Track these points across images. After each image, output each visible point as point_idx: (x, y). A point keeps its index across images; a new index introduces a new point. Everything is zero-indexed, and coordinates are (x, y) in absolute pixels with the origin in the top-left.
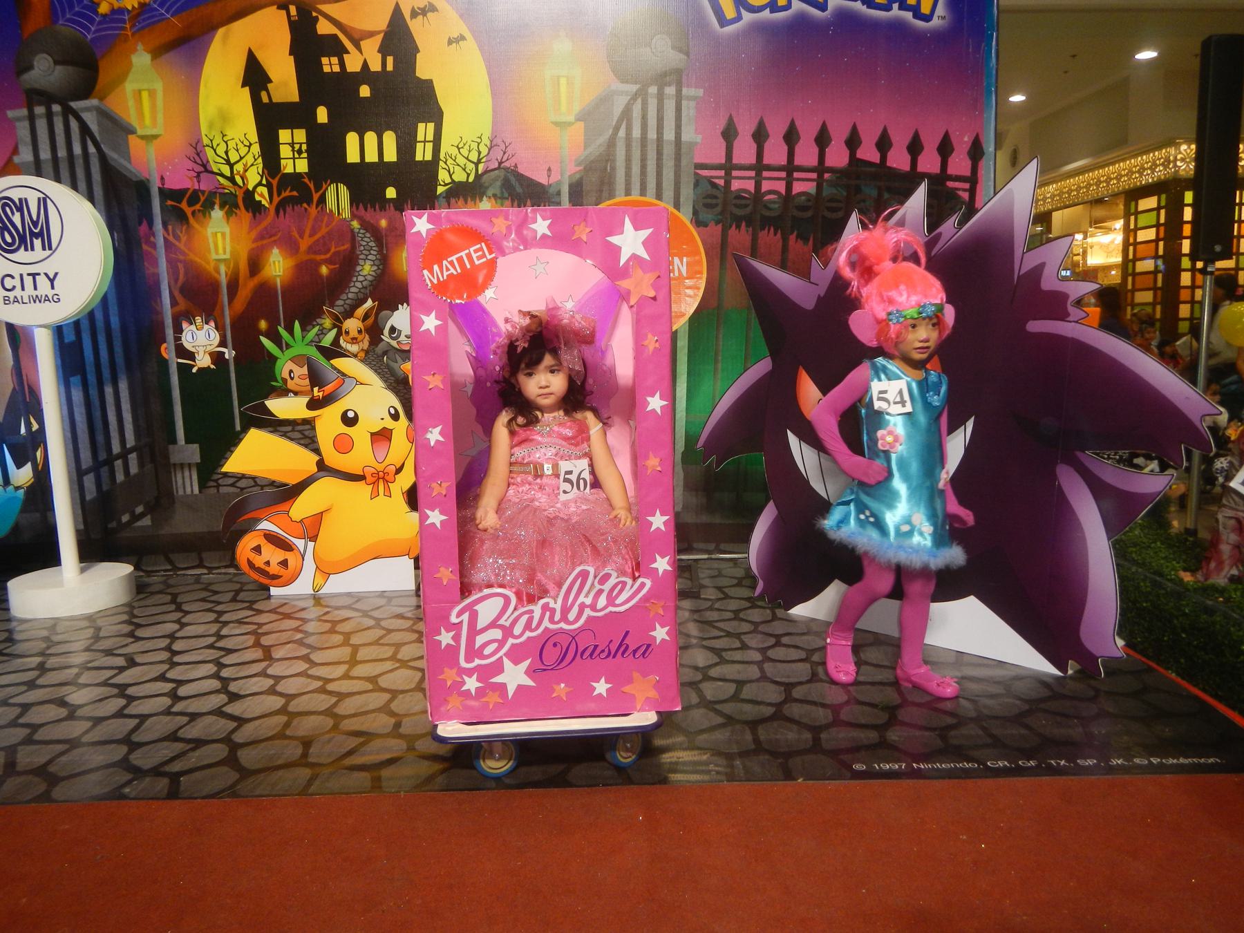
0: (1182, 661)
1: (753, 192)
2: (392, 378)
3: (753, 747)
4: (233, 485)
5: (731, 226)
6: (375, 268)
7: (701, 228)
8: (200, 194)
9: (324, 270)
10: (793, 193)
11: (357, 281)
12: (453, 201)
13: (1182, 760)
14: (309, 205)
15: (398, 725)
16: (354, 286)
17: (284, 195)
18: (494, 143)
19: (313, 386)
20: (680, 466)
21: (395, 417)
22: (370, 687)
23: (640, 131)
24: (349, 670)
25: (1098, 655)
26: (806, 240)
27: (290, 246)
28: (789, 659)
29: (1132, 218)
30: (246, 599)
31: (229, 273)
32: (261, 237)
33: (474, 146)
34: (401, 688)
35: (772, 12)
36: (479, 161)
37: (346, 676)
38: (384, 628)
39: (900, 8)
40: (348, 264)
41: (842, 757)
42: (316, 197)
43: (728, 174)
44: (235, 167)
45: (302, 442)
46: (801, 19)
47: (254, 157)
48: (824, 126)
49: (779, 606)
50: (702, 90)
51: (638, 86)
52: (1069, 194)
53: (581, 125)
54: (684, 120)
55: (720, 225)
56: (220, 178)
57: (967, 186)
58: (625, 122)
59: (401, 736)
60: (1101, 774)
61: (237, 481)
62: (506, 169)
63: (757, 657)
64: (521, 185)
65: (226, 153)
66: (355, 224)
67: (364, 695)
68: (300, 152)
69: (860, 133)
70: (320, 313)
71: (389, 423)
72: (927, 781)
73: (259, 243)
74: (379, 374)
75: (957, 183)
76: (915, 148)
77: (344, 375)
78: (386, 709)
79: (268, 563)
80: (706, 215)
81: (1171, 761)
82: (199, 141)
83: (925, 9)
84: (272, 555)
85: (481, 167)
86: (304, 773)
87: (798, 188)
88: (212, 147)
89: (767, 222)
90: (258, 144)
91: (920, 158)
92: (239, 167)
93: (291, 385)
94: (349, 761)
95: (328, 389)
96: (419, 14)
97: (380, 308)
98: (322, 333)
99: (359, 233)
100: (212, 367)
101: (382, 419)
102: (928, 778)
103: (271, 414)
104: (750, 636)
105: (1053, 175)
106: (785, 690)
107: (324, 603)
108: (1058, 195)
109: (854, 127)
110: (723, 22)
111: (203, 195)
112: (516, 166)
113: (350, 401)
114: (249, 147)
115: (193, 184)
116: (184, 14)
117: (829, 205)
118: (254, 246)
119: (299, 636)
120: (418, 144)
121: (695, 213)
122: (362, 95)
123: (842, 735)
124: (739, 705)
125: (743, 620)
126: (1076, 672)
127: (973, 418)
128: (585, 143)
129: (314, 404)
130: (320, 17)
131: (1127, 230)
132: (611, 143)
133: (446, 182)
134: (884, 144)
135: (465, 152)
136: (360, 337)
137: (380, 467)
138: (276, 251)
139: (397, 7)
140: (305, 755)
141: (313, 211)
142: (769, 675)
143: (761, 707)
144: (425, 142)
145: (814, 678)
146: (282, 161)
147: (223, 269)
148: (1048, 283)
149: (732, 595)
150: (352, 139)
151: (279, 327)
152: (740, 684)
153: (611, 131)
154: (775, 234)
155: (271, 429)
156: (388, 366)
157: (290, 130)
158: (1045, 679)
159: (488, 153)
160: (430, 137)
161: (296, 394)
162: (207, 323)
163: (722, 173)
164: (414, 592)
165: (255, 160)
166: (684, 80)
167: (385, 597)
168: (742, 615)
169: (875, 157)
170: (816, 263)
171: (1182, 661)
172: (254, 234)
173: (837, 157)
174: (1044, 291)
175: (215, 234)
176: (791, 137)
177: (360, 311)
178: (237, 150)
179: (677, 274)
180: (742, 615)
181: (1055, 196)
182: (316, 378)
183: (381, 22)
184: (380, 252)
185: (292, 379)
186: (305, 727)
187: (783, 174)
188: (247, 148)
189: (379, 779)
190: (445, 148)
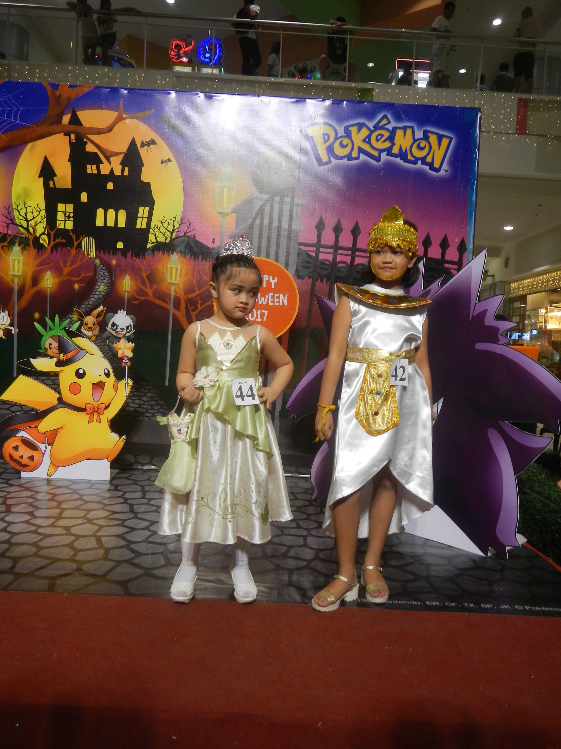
1: (331, 261)
4: (8, 409)
5: (317, 280)
6: (107, 288)
7: (301, 280)
8: (8, 236)
9: (76, 286)
10: (355, 263)
11: (95, 294)
12: (156, 253)
13: (543, 608)
14: (71, 249)
15: (75, 555)
16: (93, 297)
17: (57, 241)
18: (183, 221)
19: (60, 353)
20: (278, 419)
21: (108, 375)
22: (65, 532)
24: (55, 522)
25: (506, 545)
27: (58, 271)
30: (6, 478)
31: (20, 283)
32: (41, 264)
33: (171, 222)
35: (348, 160)
36: (173, 231)
37: (52, 525)
38: (83, 500)
39: (422, 163)
40: (91, 284)
42: (76, 243)
43: (318, 250)
44: (30, 223)
45: (53, 387)
46: (365, 165)
47: (42, 218)
50: (305, 201)
51: (269, 196)
53: (235, 215)
54: (294, 217)
55: (311, 279)
56: (20, 228)
57: (456, 267)
58: (259, 216)
59: (75, 561)
61: (11, 407)
62: (189, 237)
65: (26, 214)
66: (97, 261)
67: (59, 537)
68: (69, 217)
70: (72, 312)
71: (104, 379)
73: (40, 268)
77: (79, 347)
78: (70, 545)
79: (21, 457)
80: (303, 272)
82: (10, 205)
83: (437, 165)
84: (24, 452)
85: (174, 235)
86: (9, 578)
87: (358, 261)
88: (18, 210)
89: (339, 279)
90: (45, 211)
91: (429, 249)
92: (32, 223)
93: (49, 352)
94: (38, 573)
95: (69, 355)
96: (146, 145)
97: (107, 312)
98: (72, 323)
99: (99, 266)
100: (4, 337)
103: (34, 368)
104: (304, 521)
107: (53, 484)
108: (531, 286)
110: (320, 163)
111: (9, 237)
112: (194, 236)
113: (80, 364)
114: (39, 212)
115: (4, 230)
116: (9, 133)
118: (37, 269)
119: (31, 500)
120: (138, 218)
121: (297, 270)
122: (108, 188)
125: (302, 512)
126: (493, 554)
127: (443, 398)
128: (236, 226)
129: (59, 364)
130: (88, 142)
132: (251, 227)
135: (165, 225)
136: (94, 328)
137: (96, 404)
138: (49, 273)
139: (133, 139)
140: (13, 567)
141: (73, 252)
142: (308, 544)
143: (299, 561)
144: (143, 217)
146: (58, 222)
147: (16, 281)
148: (490, 320)
149: (298, 497)
150: (100, 213)
151: (46, 318)
152: (290, 547)
155: (35, 377)
156: (109, 346)
157: (64, 204)
159: (179, 227)
160: (146, 215)
161: (52, 357)
162: (3, 312)
163: (314, 249)
165: (42, 219)
166: (296, 195)
168: (302, 509)
171: (556, 551)
172: (36, 262)
174: (485, 325)
175: (14, 260)
177: (96, 312)
178: (32, 213)
179: (281, 304)
180: (302, 509)
181: (529, 286)
182: (62, 348)
183: (123, 147)
184: (110, 278)
185: (51, 349)
186: (16, 552)
187: (350, 253)
188: (38, 212)
190: (155, 221)
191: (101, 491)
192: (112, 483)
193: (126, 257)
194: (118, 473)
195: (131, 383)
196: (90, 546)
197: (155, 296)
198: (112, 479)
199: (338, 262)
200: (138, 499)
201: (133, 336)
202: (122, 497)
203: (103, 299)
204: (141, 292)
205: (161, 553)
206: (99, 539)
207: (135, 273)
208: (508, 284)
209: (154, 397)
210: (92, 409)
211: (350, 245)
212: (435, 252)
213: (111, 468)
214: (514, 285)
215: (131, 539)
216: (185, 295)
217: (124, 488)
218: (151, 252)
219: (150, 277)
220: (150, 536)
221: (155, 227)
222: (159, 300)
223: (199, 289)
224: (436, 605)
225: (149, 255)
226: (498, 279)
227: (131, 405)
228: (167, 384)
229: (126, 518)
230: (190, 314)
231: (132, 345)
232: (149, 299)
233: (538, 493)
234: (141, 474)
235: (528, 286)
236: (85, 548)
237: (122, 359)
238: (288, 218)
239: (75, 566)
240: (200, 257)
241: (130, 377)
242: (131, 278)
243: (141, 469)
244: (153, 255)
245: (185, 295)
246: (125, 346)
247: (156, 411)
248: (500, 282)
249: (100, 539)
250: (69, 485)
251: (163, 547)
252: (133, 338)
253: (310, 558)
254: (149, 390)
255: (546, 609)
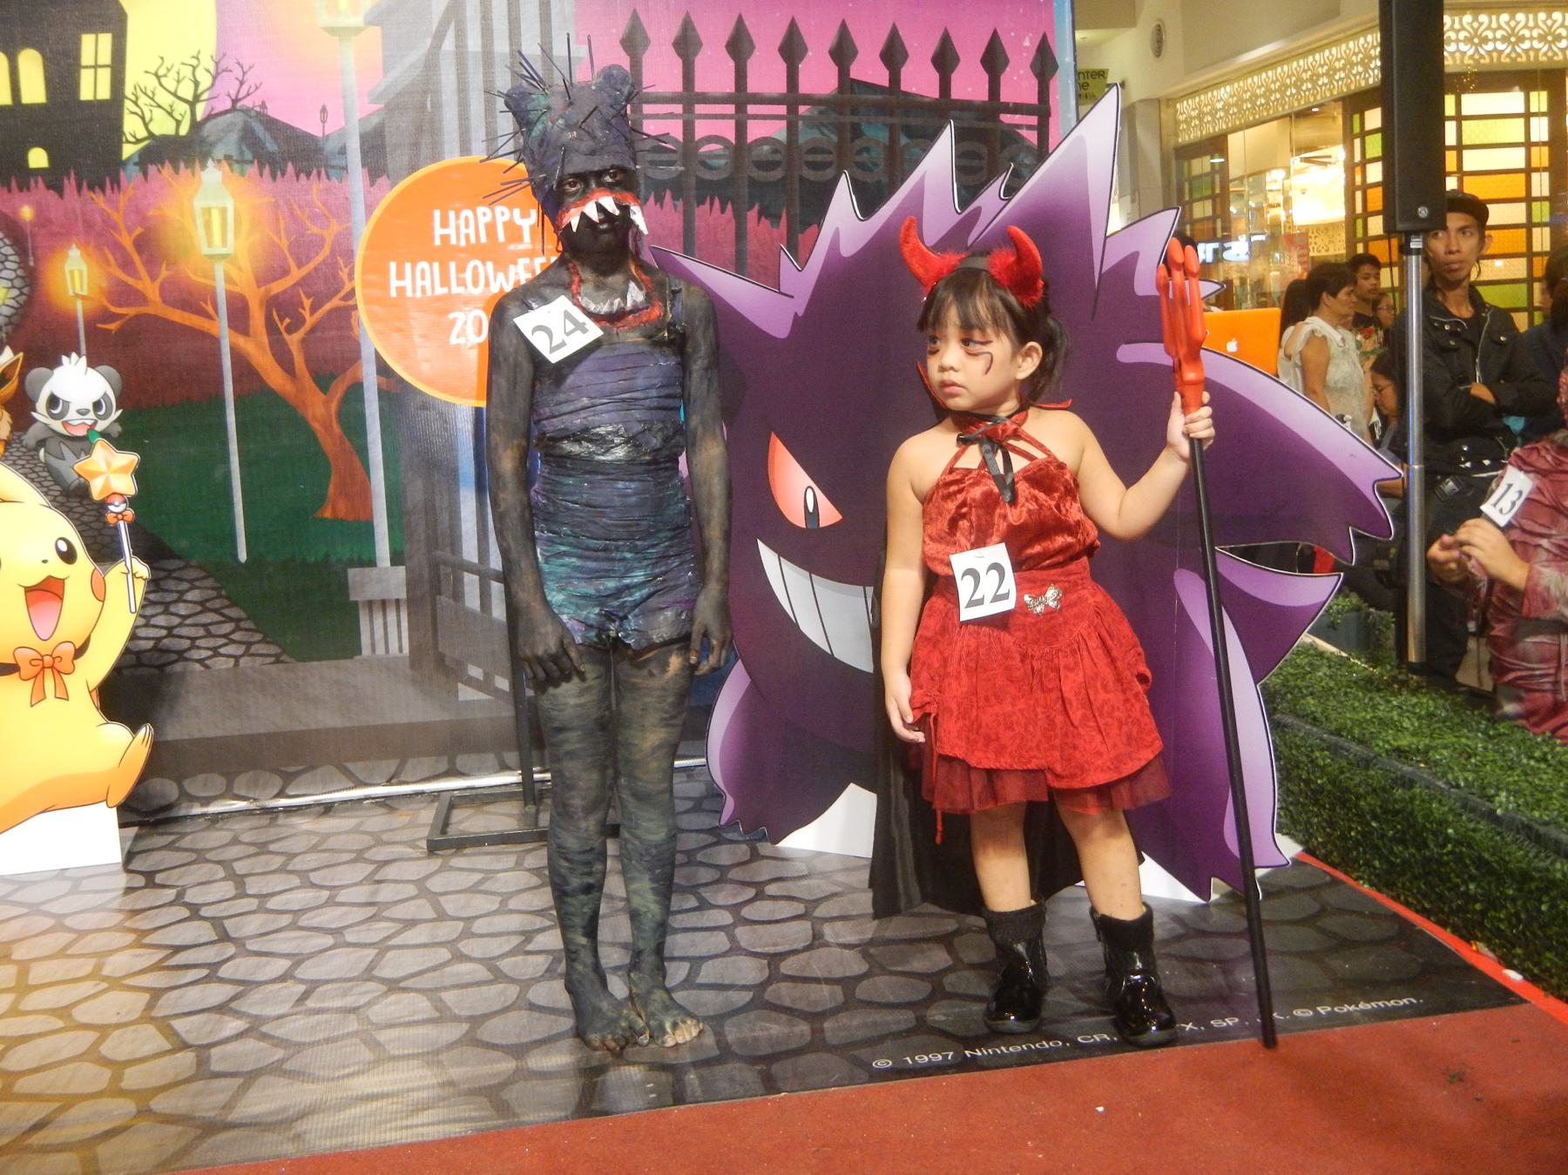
0: (1377, 863)
1: (680, 138)
2: (58, 488)
3: (717, 1052)
6: (15, 292)
10: (749, 141)
12: (152, 169)
13: (1362, 1006)
15: (117, 1078)
18: (223, 65)
21: (69, 556)
22: (60, 1024)
23: (479, 42)
24: (17, 1001)
26: (775, 218)
28: (778, 917)
29: (1357, 142)
33: (187, 71)
34: (114, 1020)
36: (197, 98)
38: (70, 930)
41: (856, 1053)
48: (793, 26)
49: (763, 838)
52: (1254, 104)
53: (376, 32)
57: (1033, 120)
60: (1244, 1037)
62: (246, 111)
63: (726, 918)
64: (275, 138)
67: (50, 1038)
69: (853, 35)
71: (58, 568)
72: (983, 1074)
74: (32, 480)
75: (1017, 116)
76: (945, 60)
78: (92, 1055)
81: (1346, 1008)
87: (755, 131)
89: (707, 190)
91: (956, 78)
94: (36, 1139)
97: (28, 365)
101: (45, 562)
102: (982, 1068)
105: (1223, 71)
106: (769, 965)
108: (1236, 105)
109: (844, 26)
112: (263, 105)
117: (810, 158)
123: (855, 1022)
124: (694, 992)
126: (1222, 896)
128: (385, 62)
131: (1350, 168)
132: (431, 64)
133: (139, 137)
134: (893, 55)
135: (170, 83)
137: (45, 648)
142: (743, 944)
143: (730, 993)
144: (96, 67)
145: (817, 941)
153: (429, 41)
154: (723, 211)
156: (47, 467)
158: (1176, 911)
159: (213, 85)
160: (105, 57)
164: (120, 867)
167: (68, 879)
169: (880, 76)
170: (787, 263)
171: (1377, 863)
173: (819, 78)
176: (739, 46)
181: (1230, 106)
184: (23, 264)
189: (95, 1159)
190: (134, 76)
191: (109, 896)
192: (131, 867)
193: (60, 190)
194: (137, 838)
195: (143, 570)
196: (148, 1049)
197: (164, 301)
198: (129, 856)
199: (701, 140)
200: (227, 900)
201: (118, 428)
202: (178, 900)
203: (10, 327)
204: (123, 294)
205: (355, 1034)
206: (164, 1025)
207: (99, 237)
208: (1168, 107)
209: (207, 600)
210: (34, 663)
211: (730, 88)
212: (969, 85)
213: (122, 825)
214: (1186, 108)
215: (254, 1011)
216: (259, 287)
217: (172, 877)
218: (137, 168)
219: (142, 244)
220: (305, 996)
221: (139, 93)
222: (184, 309)
223: (300, 265)
224: (1103, 1040)
225: (131, 175)
226: (1137, 93)
227: (142, 633)
228: (243, 556)
229: (217, 960)
230: (284, 343)
231: (130, 459)
232: (150, 310)
233: (1315, 721)
234: (203, 830)
235: (1226, 109)
236: (138, 1055)
237: (103, 506)
238: (537, 26)
239: (128, 1107)
240: (290, 168)
241: (139, 552)
242: (87, 255)
243: (203, 815)
244: (145, 174)
245: (259, 287)
246: (109, 465)
247: (224, 641)
248: (1145, 101)
249: (172, 1028)
250: (9, 894)
251: (352, 1016)
252: (121, 435)
253: (758, 982)
254: (191, 581)
255: (1368, 1006)
